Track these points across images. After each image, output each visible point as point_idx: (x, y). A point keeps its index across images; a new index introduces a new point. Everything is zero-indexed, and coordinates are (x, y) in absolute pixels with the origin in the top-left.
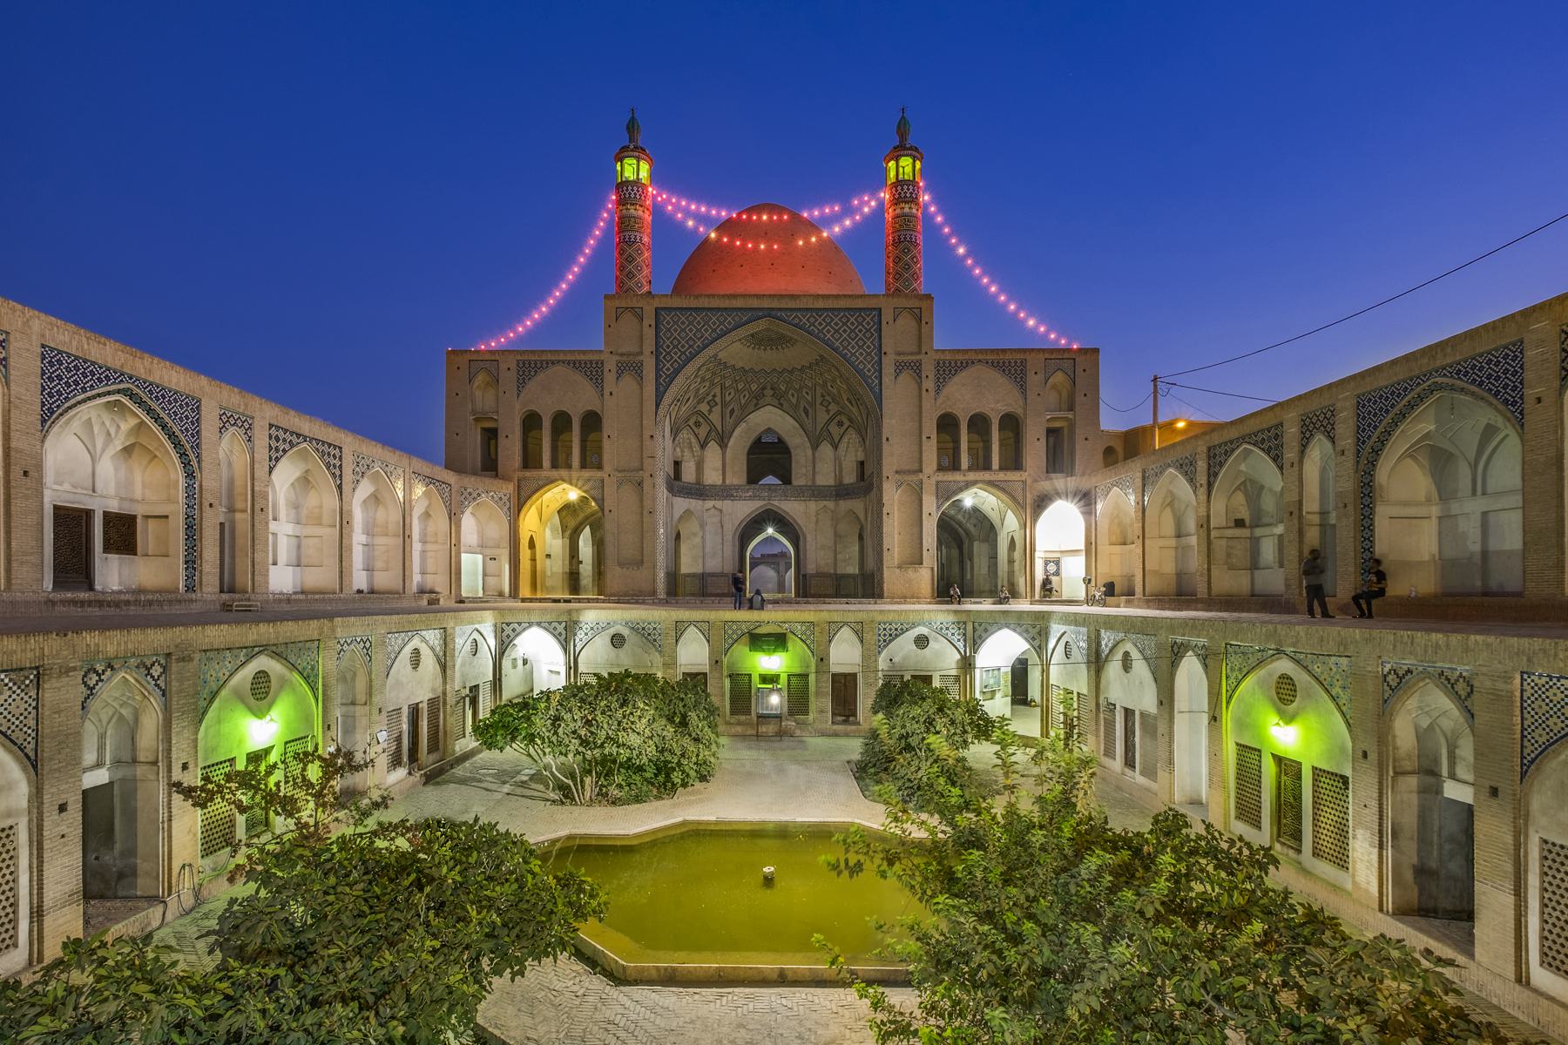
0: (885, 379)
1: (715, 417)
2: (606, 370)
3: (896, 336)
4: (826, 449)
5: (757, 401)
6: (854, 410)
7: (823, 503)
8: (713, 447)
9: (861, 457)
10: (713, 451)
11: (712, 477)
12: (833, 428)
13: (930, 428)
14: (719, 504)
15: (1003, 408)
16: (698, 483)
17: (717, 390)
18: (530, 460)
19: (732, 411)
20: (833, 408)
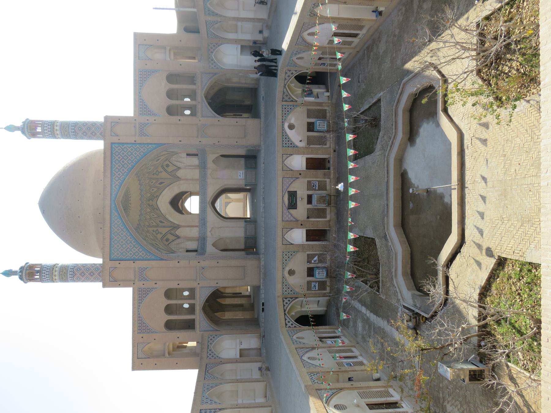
0: (149, 141)
4: (180, 173)
5: (155, 209)
6: (162, 158)
8: (179, 232)
9: (184, 155)
11: (195, 232)
12: (170, 169)
14: (209, 229)
15: (164, 82)
16: (198, 240)
17: (151, 229)
18: (189, 325)
19: (161, 222)
20: (160, 169)
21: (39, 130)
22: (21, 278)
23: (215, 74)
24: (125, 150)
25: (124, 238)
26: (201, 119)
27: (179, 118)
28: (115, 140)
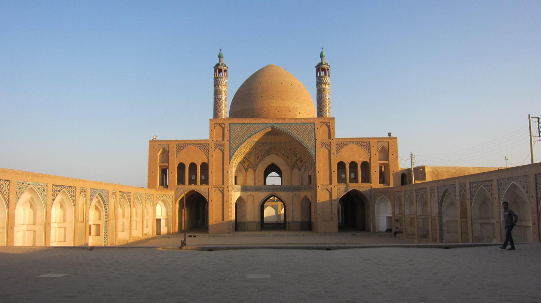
1: (251, 160)
2: (210, 147)
3: (321, 134)
4: (296, 171)
5: (268, 153)
6: (306, 158)
7: (294, 193)
9: (310, 174)
10: (250, 172)
11: (250, 182)
12: (299, 163)
13: (335, 168)
14: (252, 193)
15: (362, 160)
18: (181, 181)
19: (258, 157)
21: (322, 73)
22: (218, 65)
23: (371, 197)
24: (310, 133)
25: (246, 133)
26: (336, 188)
27: (336, 171)
28: (317, 126)
